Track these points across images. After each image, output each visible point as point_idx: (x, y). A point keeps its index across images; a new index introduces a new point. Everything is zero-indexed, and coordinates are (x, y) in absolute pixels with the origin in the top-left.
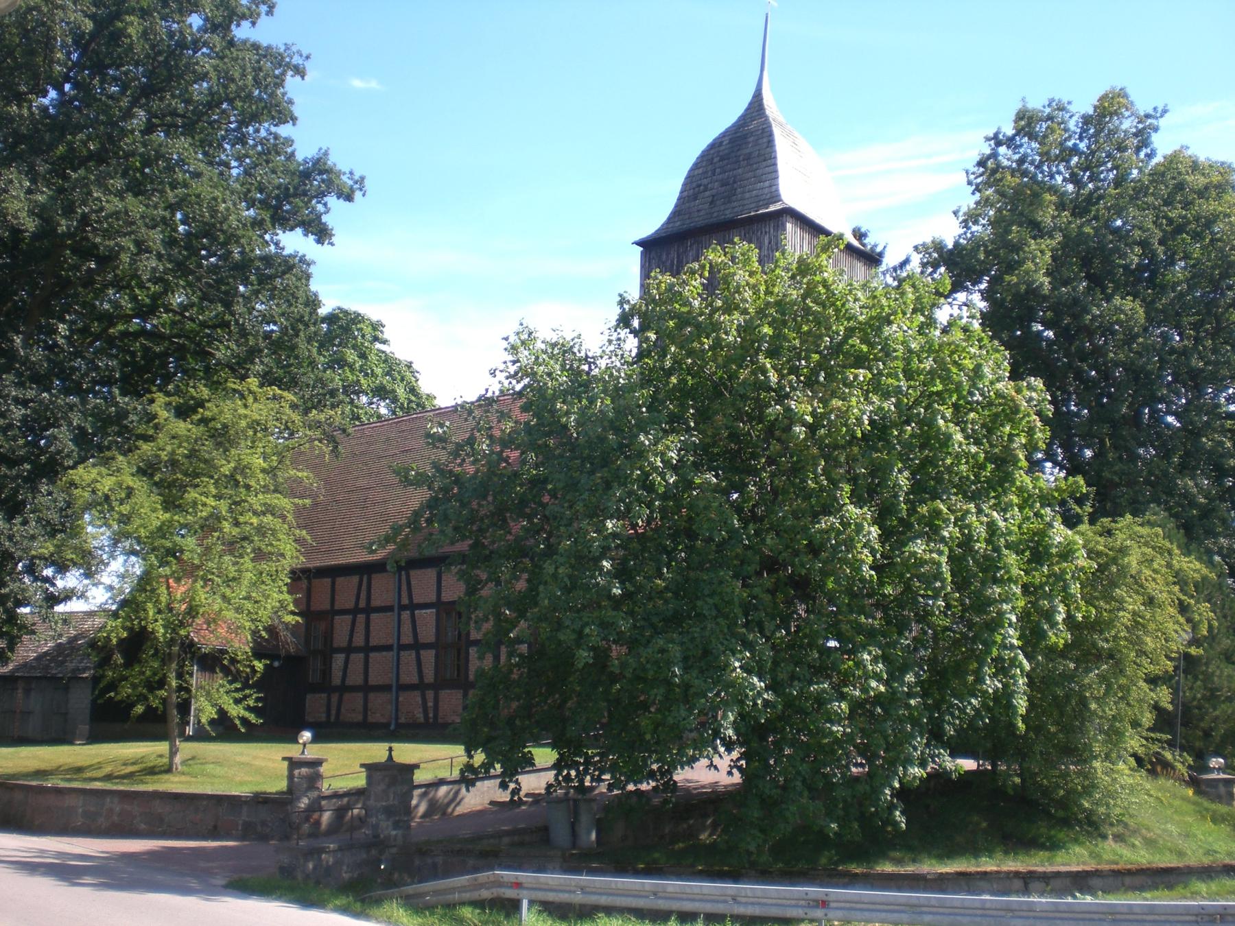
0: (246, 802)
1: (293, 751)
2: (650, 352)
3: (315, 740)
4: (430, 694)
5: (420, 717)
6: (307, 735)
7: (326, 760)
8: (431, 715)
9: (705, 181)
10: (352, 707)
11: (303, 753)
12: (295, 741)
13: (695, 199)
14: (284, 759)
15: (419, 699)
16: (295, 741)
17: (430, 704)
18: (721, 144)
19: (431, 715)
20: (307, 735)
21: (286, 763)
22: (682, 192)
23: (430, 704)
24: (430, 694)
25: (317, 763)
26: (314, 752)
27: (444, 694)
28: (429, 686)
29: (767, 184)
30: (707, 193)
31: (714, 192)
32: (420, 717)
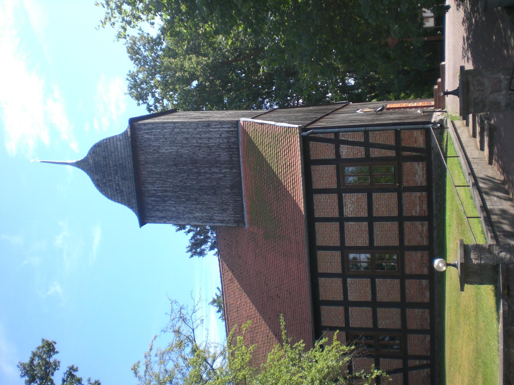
0: (509, 308)
1: (452, 277)
2: (162, 62)
3: (442, 254)
4: (411, 363)
5: (427, 371)
6: (438, 263)
7: (462, 241)
8: (425, 362)
9: (114, 185)
10: (417, 318)
11: (455, 266)
12: (443, 273)
13: (122, 191)
14: (462, 289)
15: (414, 372)
16: (443, 273)
17: (417, 362)
18: (98, 180)
19: (425, 362)
20: (438, 263)
21: (467, 286)
22: (119, 202)
23: (417, 362)
24: (411, 363)
25: (466, 249)
26: (454, 254)
27: (411, 351)
28: (405, 363)
29: (119, 143)
30: (121, 183)
31: (120, 179)
32: (427, 371)
